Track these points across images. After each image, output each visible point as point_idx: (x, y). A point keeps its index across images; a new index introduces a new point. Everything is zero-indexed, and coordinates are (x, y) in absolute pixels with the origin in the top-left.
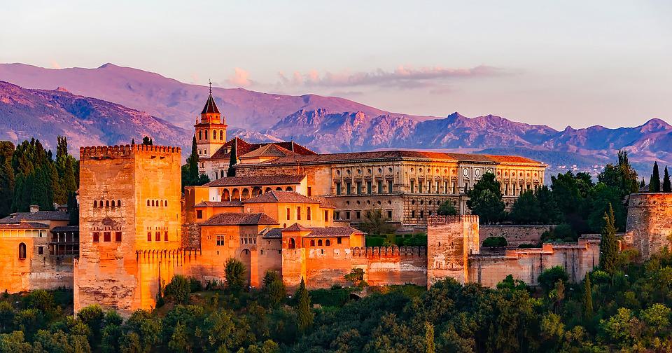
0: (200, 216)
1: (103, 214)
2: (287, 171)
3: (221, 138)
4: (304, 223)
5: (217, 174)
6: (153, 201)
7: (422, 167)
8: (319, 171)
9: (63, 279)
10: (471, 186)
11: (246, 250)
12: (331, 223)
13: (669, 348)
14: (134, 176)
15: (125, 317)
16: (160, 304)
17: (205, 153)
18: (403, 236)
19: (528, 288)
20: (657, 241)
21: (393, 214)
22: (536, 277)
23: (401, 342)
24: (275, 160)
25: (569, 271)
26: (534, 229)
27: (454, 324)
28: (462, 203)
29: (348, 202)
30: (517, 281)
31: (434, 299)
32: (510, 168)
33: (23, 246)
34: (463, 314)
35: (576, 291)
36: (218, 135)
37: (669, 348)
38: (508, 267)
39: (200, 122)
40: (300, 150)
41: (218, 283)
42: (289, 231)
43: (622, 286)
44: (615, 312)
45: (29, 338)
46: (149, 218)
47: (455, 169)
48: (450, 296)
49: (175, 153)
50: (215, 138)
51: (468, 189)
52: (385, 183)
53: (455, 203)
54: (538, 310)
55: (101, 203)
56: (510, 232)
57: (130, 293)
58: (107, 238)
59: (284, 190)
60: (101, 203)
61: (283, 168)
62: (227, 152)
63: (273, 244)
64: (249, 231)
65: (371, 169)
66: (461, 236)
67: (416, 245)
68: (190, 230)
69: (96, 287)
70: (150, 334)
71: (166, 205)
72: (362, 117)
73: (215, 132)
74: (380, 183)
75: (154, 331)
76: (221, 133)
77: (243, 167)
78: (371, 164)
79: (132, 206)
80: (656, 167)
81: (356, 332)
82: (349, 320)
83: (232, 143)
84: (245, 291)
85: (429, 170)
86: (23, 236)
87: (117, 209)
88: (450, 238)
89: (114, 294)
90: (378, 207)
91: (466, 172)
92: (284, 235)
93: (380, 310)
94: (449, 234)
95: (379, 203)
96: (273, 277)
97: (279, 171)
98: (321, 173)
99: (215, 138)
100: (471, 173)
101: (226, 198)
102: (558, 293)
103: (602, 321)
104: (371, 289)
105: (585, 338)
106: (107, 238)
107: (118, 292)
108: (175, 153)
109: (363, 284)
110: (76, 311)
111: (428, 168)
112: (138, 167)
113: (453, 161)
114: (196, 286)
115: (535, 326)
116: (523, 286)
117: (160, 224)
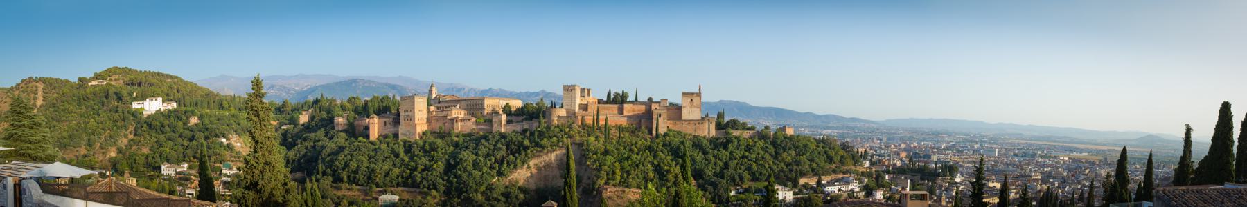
1: (406, 114)
4: (459, 116)
16: (421, 138)
35: (532, 134)
45: (388, 146)
54: (522, 139)
67: (489, 122)
79: (414, 113)
86: (385, 120)
116: (517, 133)
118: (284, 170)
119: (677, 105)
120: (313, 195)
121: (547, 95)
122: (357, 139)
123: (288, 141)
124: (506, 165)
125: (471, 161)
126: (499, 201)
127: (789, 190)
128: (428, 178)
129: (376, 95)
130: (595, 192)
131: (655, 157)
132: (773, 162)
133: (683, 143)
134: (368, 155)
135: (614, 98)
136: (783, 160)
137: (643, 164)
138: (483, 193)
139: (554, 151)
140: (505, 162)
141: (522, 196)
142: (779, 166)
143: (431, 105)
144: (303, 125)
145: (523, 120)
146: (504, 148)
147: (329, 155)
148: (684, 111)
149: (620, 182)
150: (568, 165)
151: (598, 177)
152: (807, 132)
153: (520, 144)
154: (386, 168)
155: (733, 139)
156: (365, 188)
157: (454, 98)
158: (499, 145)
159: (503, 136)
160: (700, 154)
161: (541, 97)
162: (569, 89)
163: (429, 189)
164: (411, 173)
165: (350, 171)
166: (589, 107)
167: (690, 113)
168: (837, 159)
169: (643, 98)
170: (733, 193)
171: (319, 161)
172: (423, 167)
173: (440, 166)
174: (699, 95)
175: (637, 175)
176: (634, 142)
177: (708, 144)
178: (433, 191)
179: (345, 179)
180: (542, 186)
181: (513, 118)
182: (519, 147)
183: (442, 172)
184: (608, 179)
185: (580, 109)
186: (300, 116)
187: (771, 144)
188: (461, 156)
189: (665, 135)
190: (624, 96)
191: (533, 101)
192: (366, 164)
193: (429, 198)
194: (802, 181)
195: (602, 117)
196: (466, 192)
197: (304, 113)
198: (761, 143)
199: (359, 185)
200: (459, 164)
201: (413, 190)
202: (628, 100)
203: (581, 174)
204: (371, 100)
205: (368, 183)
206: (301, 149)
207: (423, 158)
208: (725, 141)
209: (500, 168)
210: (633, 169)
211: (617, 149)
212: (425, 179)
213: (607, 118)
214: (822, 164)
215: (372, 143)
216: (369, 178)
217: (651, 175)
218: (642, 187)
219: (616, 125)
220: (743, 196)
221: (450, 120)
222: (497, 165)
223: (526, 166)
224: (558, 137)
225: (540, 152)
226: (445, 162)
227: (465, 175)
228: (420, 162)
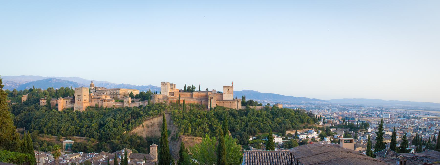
4: (106, 98)
9: (72, 106)
10: (129, 93)
12: (110, 98)
15: (81, 111)
16: (86, 110)
22: (139, 106)
25: (143, 105)
33: (67, 102)
34: (129, 111)
35: (144, 108)
42: (104, 99)
43: (151, 107)
44: (150, 111)
45: (68, 114)
52: (117, 93)
54: (139, 111)
58: (79, 100)
64: (98, 99)
67: (122, 101)
69: (77, 107)
79: (82, 96)
86: (67, 100)
90: (116, 96)
91: (128, 91)
96: (102, 106)
102: (142, 108)
104: (116, 108)
105: (146, 115)
106: (79, 100)
109: (114, 107)
110: (74, 110)
114: (91, 107)
116: (137, 107)
118: (12, 126)
119: (221, 93)
120: (28, 140)
121: (153, 87)
122: (52, 110)
123: (15, 111)
124: (131, 124)
125: (112, 122)
126: (127, 144)
127: (280, 138)
128: (89, 131)
129: (62, 87)
130: (178, 139)
131: (209, 120)
132: (271, 123)
133: (224, 112)
134: (57, 119)
135: (188, 89)
136: (277, 121)
137: (203, 124)
138: (118, 139)
139: (156, 117)
140: (130, 123)
141: (139, 141)
142: (275, 125)
143: (91, 93)
144: (24, 102)
145: (139, 100)
146: (130, 115)
147: (37, 119)
148: (224, 95)
149: (191, 134)
150: (164, 124)
151: (179, 131)
152: (289, 106)
153: (138, 113)
154: (67, 126)
155: (251, 110)
156: (56, 137)
157: (104, 89)
158: (127, 114)
159: (129, 109)
160: (233, 118)
161: (149, 88)
162: (164, 84)
163: (90, 137)
164: (80, 129)
165: (48, 127)
166: (174, 94)
167: (226, 97)
168: (305, 120)
169: (203, 89)
170: (251, 139)
171: (32, 122)
172: (87, 126)
173: (95, 125)
174: (232, 87)
175: (200, 130)
176: (198, 112)
177: (237, 113)
178: (92, 138)
179: (46, 131)
180: (150, 136)
181: (134, 100)
182: (137, 115)
183: (96, 128)
184: (185, 132)
185: (170, 95)
186: (22, 98)
187: (270, 113)
188: (107, 120)
189: (215, 108)
190: (193, 88)
191: (145, 91)
192: (56, 123)
193: (90, 142)
194: (287, 133)
195: (182, 99)
196: (109, 139)
197: (24, 96)
198: (265, 112)
199: (53, 135)
201: (81, 137)
202: (195, 90)
203: (170, 130)
204: (59, 90)
205: (58, 134)
206: (22, 115)
207: (86, 121)
208: (246, 111)
209: (127, 126)
210: (198, 126)
211: (189, 116)
212: (87, 132)
213: (184, 100)
214: (298, 123)
215: (60, 112)
216: (58, 131)
217: (207, 129)
218: (203, 136)
219: (189, 103)
220: (256, 141)
221: (101, 101)
222: (126, 125)
223: (141, 125)
224: (158, 110)
225: (149, 117)
226: (99, 123)
227: (109, 130)
228: (85, 123)
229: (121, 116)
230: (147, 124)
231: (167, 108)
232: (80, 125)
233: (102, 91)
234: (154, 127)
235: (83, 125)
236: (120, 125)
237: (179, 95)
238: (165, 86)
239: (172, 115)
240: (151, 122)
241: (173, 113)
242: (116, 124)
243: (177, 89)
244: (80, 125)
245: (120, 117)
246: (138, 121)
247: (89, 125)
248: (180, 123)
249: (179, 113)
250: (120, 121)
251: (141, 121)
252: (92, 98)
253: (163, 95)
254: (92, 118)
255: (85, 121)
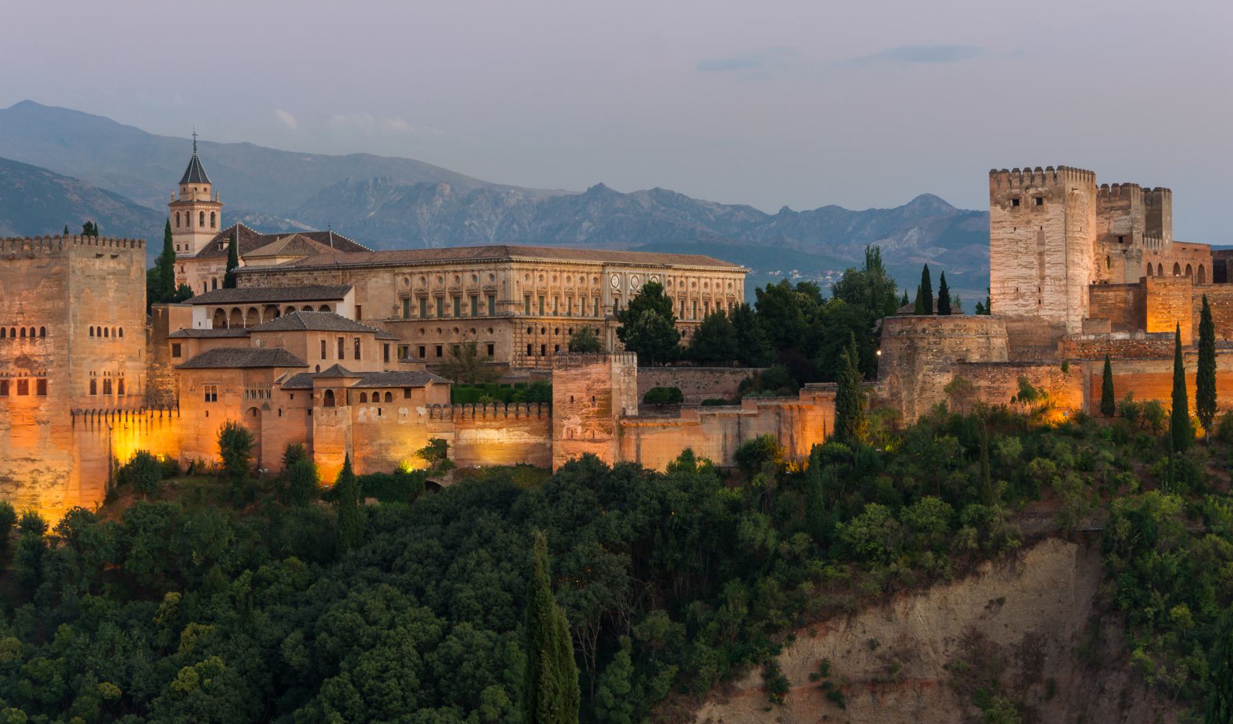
0: (177, 352)
2: (321, 279)
3: (213, 225)
4: (350, 365)
5: (205, 284)
6: (99, 329)
7: (544, 274)
8: (374, 280)
10: (624, 304)
11: (255, 409)
12: (395, 365)
13: (948, 568)
14: (67, 288)
17: (187, 248)
18: (513, 386)
19: (718, 471)
20: (928, 394)
21: (496, 350)
22: (731, 452)
23: (510, 560)
24: (302, 261)
26: (727, 375)
27: (597, 531)
28: (609, 332)
29: (423, 331)
30: (699, 459)
31: (563, 489)
32: (688, 274)
36: (207, 219)
37: (948, 568)
38: (686, 437)
39: (177, 197)
40: (343, 245)
41: (208, 464)
44: (860, 510)
46: (94, 357)
47: (598, 276)
48: (591, 484)
49: (136, 248)
50: (202, 223)
51: (619, 309)
52: (483, 298)
53: (598, 331)
54: (734, 507)
55: (13, 331)
56: (687, 379)
57: (61, 481)
58: (23, 389)
59: (316, 311)
60: (13, 331)
61: (316, 274)
62: (222, 248)
63: (300, 399)
64: (258, 377)
65: (460, 275)
66: (607, 386)
68: (162, 376)
70: (93, 547)
71: (121, 335)
72: (447, 190)
73: (202, 215)
74: (474, 298)
75: (101, 543)
76: (213, 215)
77: (250, 273)
78: (459, 268)
79: (64, 341)
80: (926, 272)
81: (435, 542)
82: (424, 524)
83: (230, 234)
84: (252, 476)
85: (555, 278)
87: (39, 341)
88: (589, 389)
89: (35, 482)
90: (472, 338)
91: (615, 281)
92: (316, 384)
93: (474, 508)
94: (587, 382)
95: (474, 331)
97: (307, 278)
98: (377, 282)
99: (202, 223)
100: (624, 282)
101: (220, 323)
103: (839, 525)
105: (811, 553)
107: (41, 479)
108: (136, 248)
109: (446, 466)
111: (552, 274)
112: (74, 272)
113: (594, 262)
115: (728, 532)
117: (112, 367)
140: (624, 656)
145: (745, 388)
146: (618, 564)
172: (111, 689)
200: (336, 672)
207: (108, 630)
223: (755, 677)
224: (955, 498)
225: (844, 585)
229: (514, 577)
230: (824, 667)
231: (1063, 469)
232: (35, 682)
233: (307, 279)
234: (909, 704)
235: (67, 678)
236: (501, 679)
237: (1206, 314)
238: (1037, 220)
239: (1114, 557)
240: (873, 645)
241: (1124, 527)
242: (460, 660)
243: (1183, 247)
244: (35, 682)
245: (508, 588)
246: (713, 625)
247: (137, 680)
248: (1206, 644)
249: (1200, 527)
250: (500, 631)
251: (755, 628)
252: (179, 361)
253: (1020, 319)
254: (172, 596)
255: (92, 631)
